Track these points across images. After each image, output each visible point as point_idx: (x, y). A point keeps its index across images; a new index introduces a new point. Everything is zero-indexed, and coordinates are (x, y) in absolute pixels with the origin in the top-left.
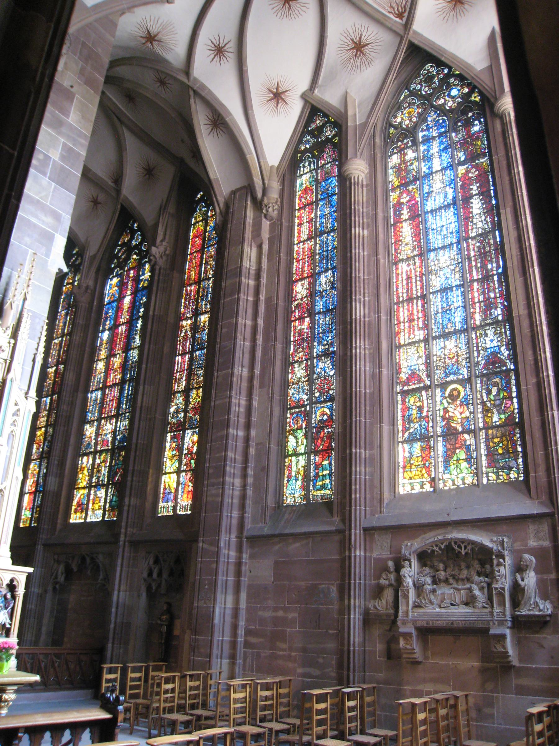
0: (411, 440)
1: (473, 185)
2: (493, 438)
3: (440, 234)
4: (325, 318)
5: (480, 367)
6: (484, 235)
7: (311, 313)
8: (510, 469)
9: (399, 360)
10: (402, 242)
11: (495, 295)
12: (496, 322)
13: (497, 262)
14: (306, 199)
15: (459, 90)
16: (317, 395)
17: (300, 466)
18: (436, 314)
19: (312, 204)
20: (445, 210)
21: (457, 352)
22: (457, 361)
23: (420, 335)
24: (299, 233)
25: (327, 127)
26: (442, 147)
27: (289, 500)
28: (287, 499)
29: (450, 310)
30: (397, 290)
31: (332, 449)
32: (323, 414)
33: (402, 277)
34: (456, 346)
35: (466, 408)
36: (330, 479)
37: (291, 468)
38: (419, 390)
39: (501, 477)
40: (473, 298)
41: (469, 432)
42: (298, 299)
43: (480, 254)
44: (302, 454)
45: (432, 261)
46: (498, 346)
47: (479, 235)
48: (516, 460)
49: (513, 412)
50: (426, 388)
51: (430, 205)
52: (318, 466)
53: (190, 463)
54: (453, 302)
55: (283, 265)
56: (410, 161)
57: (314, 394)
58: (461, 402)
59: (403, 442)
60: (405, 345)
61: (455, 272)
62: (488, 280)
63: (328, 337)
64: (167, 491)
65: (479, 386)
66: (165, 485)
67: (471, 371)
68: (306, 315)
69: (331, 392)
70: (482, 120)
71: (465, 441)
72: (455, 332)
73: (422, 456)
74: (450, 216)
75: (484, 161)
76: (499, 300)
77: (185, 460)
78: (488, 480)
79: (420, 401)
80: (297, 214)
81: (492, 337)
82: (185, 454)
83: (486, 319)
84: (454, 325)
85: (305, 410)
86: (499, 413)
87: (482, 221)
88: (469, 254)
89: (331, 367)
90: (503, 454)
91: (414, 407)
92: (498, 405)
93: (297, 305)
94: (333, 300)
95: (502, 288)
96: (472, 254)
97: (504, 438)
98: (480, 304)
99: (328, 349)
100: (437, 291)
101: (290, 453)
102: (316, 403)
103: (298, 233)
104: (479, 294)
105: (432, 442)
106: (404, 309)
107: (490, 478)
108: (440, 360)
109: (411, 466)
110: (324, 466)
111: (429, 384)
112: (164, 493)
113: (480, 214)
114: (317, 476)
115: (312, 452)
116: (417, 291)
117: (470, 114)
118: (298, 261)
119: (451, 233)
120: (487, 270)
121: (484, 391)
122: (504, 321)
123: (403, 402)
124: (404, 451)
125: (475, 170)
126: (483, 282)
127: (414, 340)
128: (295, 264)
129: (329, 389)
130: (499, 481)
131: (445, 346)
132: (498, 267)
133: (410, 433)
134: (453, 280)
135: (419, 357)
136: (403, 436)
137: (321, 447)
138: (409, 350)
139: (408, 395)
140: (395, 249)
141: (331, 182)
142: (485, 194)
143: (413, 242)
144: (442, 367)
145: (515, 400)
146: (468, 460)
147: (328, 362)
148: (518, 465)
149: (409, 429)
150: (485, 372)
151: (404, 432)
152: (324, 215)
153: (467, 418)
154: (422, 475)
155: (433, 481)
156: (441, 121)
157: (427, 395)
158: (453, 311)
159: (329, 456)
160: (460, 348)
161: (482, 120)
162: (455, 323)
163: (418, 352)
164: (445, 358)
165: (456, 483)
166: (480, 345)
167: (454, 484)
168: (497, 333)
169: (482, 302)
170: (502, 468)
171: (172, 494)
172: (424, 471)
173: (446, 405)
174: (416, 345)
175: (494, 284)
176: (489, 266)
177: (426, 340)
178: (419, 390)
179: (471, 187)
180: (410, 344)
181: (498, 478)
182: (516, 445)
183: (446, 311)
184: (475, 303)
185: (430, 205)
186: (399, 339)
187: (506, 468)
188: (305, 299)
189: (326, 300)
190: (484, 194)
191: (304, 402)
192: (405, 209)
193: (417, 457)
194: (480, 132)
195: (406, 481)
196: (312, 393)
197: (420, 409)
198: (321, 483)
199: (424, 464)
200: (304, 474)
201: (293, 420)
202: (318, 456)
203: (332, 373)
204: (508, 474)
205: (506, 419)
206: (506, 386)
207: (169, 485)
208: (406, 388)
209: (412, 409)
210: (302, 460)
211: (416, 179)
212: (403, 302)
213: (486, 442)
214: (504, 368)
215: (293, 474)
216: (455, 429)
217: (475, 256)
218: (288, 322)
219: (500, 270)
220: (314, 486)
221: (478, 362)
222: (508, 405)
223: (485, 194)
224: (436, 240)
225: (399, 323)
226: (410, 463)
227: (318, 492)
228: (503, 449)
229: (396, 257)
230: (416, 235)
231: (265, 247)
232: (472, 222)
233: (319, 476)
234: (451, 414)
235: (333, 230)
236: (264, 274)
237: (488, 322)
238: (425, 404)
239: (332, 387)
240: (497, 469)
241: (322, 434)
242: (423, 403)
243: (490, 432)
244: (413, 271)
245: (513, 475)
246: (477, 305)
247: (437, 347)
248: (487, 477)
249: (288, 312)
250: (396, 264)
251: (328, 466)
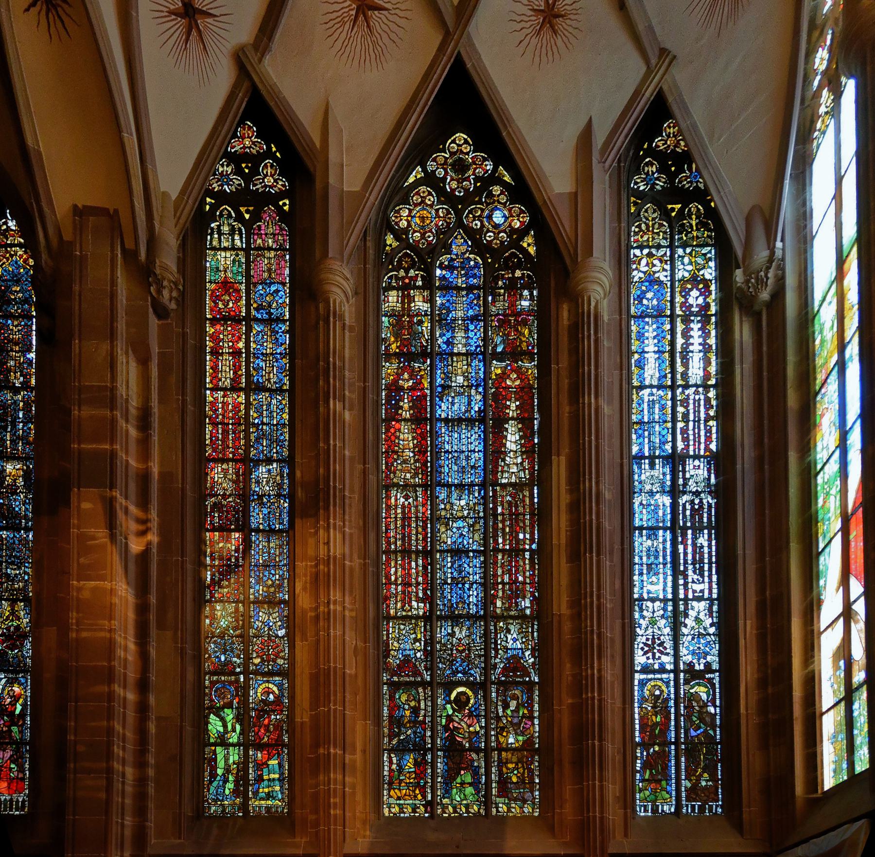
0: (401, 750)
1: (510, 400)
2: (507, 763)
3: (456, 464)
4: (269, 542)
5: (499, 671)
6: (518, 486)
7: (245, 528)
8: (524, 801)
9: (388, 634)
10: (398, 456)
11: (525, 579)
12: (522, 617)
13: (532, 534)
14: (226, 305)
15: (506, 218)
16: (257, 661)
17: (231, 761)
18: (443, 584)
19: (239, 322)
20: (467, 426)
21: (469, 644)
22: (468, 656)
23: (418, 608)
24: (215, 368)
25: (266, 166)
26: (471, 313)
27: (213, 808)
28: (209, 808)
29: (463, 584)
30: (386, 532)
31: (284, 745)
32: (268, 692)
33: (396, 514)
34: (469, 636)
35: (475, 721)
36: (281, 787)
37: (216, 763)
38: (416, 685)
39: (513, 810)
40: (495, 575)
41: (478, 751)
42: (216, 495)
43: (511, 514)
44: (233, 745)
45: (442, 501)
46: (522, 649)
47: (510, 484)
48: (532, 792)
49: (532, 736)
50: (424, 684)
51: (444, 410)
52: (261, 766)
54: (469, 573)
56: (417, 315)
57: (252, 658)
58: (470, 712)
59: (390, 751)
60: (396, 617)
61: (474, 530)
62: (517, 556)
63: (273, 575)
65: (494, 695)
67: (486, 675)
68: (233, 527)
69: (280, 661)
70: (535, 293)
71: (473, 760)
72: (469, 616)
73: (415, 772)
74: (473, 438)
75: (530, 367)
76: (528, 587)
78: (498, 811)
79: (414, 699)
80: (210, 330)
81: (515, 635)
83: (509, 609)
84: (466, 606)
85: (237, 681)
86: (516, 734)
87: (517, 464)
88: (495, 509)
89: (280, 623)
90: (517, 782)
91: (407, 707)
92: (516, 724)
93: (215, 503)
94: (280, 515)
95: (534, 572)
96: (500, 510)
97: (520, 765)
98: (503, 586)
99: (274, 593)
100: (447, 551)
101: (212, 740)
102: (256, 673)
103: (212, 368)
104: (503, 572)
105: (429, 756)
106: (396, 563)
107: (500, 809)
108: (445, 650)
109: (400, 783)
110: (270, 767)
111: (428, 680)
113: (516, 452)
114: (260, 779)
115: (251, 745)
116: (417, 544)
117: (518, 273)
118: (215, 424)
119: (473, 467)
120: (518, 541)
121: (500, 703)
122: (532, 618)
123: (392, 698)
124: (391, 762)
125: (515, 376)
126: (510, 556)
127: (410, 614)
128: (209, 428)
129: (277, 656)
130: (511, 814)
131: (454, 632)
132: (532, 541)
133: (399, 740)
134: (471, 541)
135: (416, 640)
136: (390, 743)
137: (266, 739)
138: (402, 627)
139: (399, 689)
140: (387, 463)
141: (277, 291)
142: (527, 422)
143: (416, 461)
144: (448, 660)
145: (536, 722)
146: (475, 784)
147: (274, 615)
148: (535, 798)
149: (398, 735)
150: (503, 679)
151: (391, 736)
152: (262, 354)
153: (477, 733)
154: (415, 796)
155: (430, 805)
156: (472, 263)
157: (425, 693)
158: (467, 586)
159: (279, 755)
160: (473, 640)
161: (535, 293)
162: (469, 605)
163: (415, 633)
164: (452, 650)
165: (458, 810)
166: (499, 642)
167: (455, 811)
168: (522, 632)
169: (507, 583)
170: (515, 800)
172: (417, 792)
173: (450, 712)
174: (413, 621)
175: (525, 564)
176: (521, 536)
177: (428, 618)
178: (416, 685)
179: (508, 403)
180: (403, 618)
181: (509, 810)
182: (533, 775)
183: (457, 584)
184: (498, 584)
185: (444, 410)
186: (388, 606)
187: (520, 800)
189: (269, 513)
190: (525, 421)
191: (235, 668)
192: (406, 401)
193: (409, 772)
194: (529, 312)
195: (392, 801)
196: (248, 659)
197: (415, 711)
198: (266, 790)
199: (419, 783)
200: (237, 774)
201: (215, 691)
202: (261, 752)
203: (282, 633)
204: (521, 808)
205: (524, 742)
206: (527, 702)
208: (395, 679)
209: (404, 709)
210: (234, 756)
211: (424, 354)
212: (395, 552)
213: (498, 766)
214: (527, 679)
215: (220, 772)
216: (460, 743)
217: (503, 514)
218: (200, 528)
219: (534, 546)
220: (256, 793)
221: (496, 664)
222: (528, 726)
223: (527, 422)
224: (450, 472)
225: (389, 583)
226: (399, 778)
227: (263, 802)
228: (518, 777)
229: (387, 477)
230: (420, 451)
232: (504, 460)
233: (263, 780)
234: (456, 725)
235: (280, 391)
237: (512, 613)
238: (422, 706)
239: (282, 654)
240: (510, 800)
241: (266, 721)
242: (419, 704)
243: (504, 754)
244: (413, 509)
245: (527, 809)
246: (500, 586)
247: (442, 632)
248: (497, 808)
249: (201, 514)
250: (388, 487)
251: (277, 767)
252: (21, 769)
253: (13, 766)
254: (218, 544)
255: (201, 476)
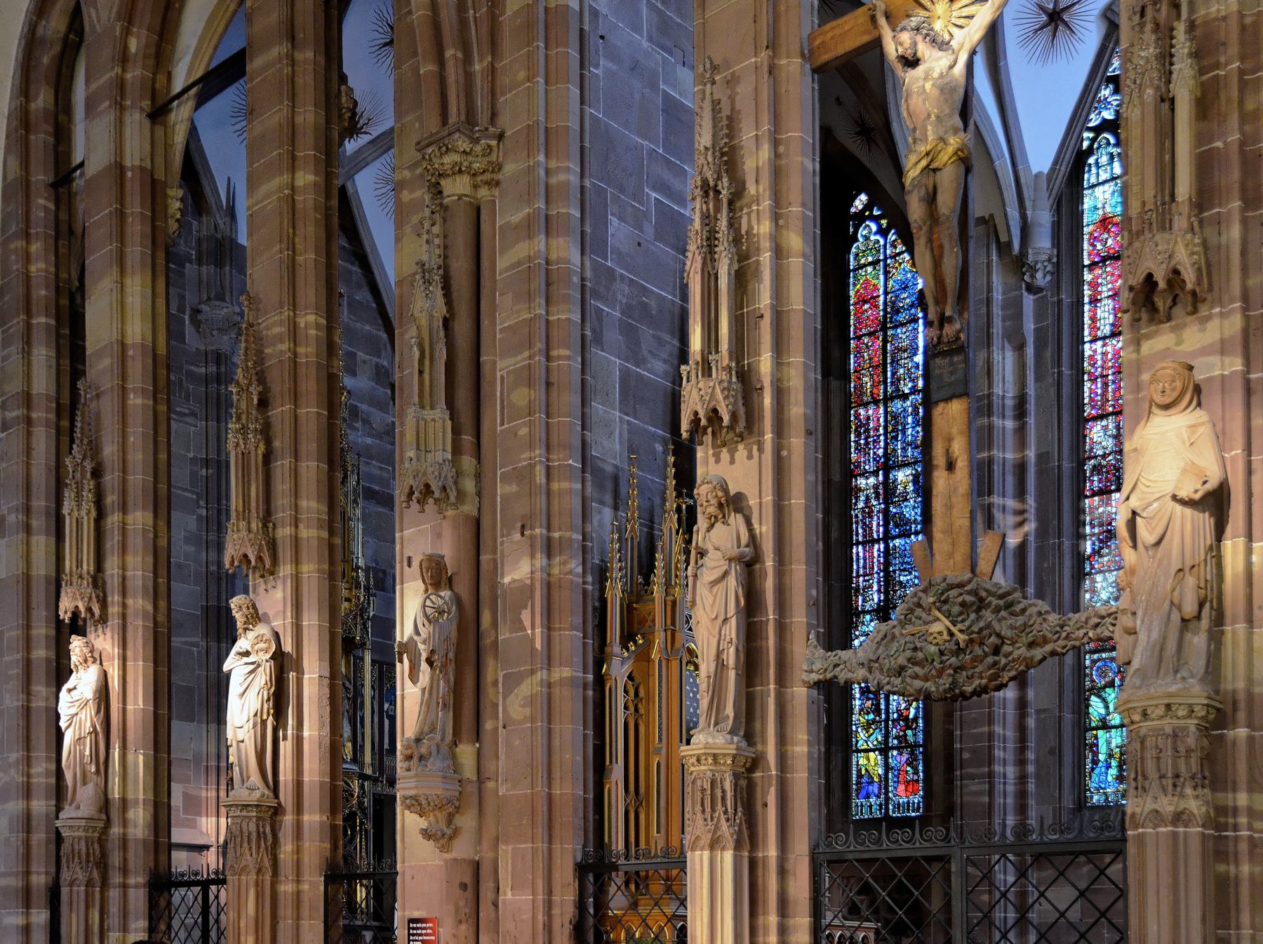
53: (905, 735)
55: (1066, 390)
64: (864, 780)
66: (859, 771)
68: (1113, 487)
77: (894, 730)
82: (894, 721)
93: (1094, 466)
112: (858, 783)
128: (1087, 385)
171: (876, 785)
188: (1111, 458)
207: (866, 770)
231: (1030, 351)
236: (1031, 407)
252: (916, 772)
253: (909, 768)
254: (1097, 509)
255: (1079, 437)
